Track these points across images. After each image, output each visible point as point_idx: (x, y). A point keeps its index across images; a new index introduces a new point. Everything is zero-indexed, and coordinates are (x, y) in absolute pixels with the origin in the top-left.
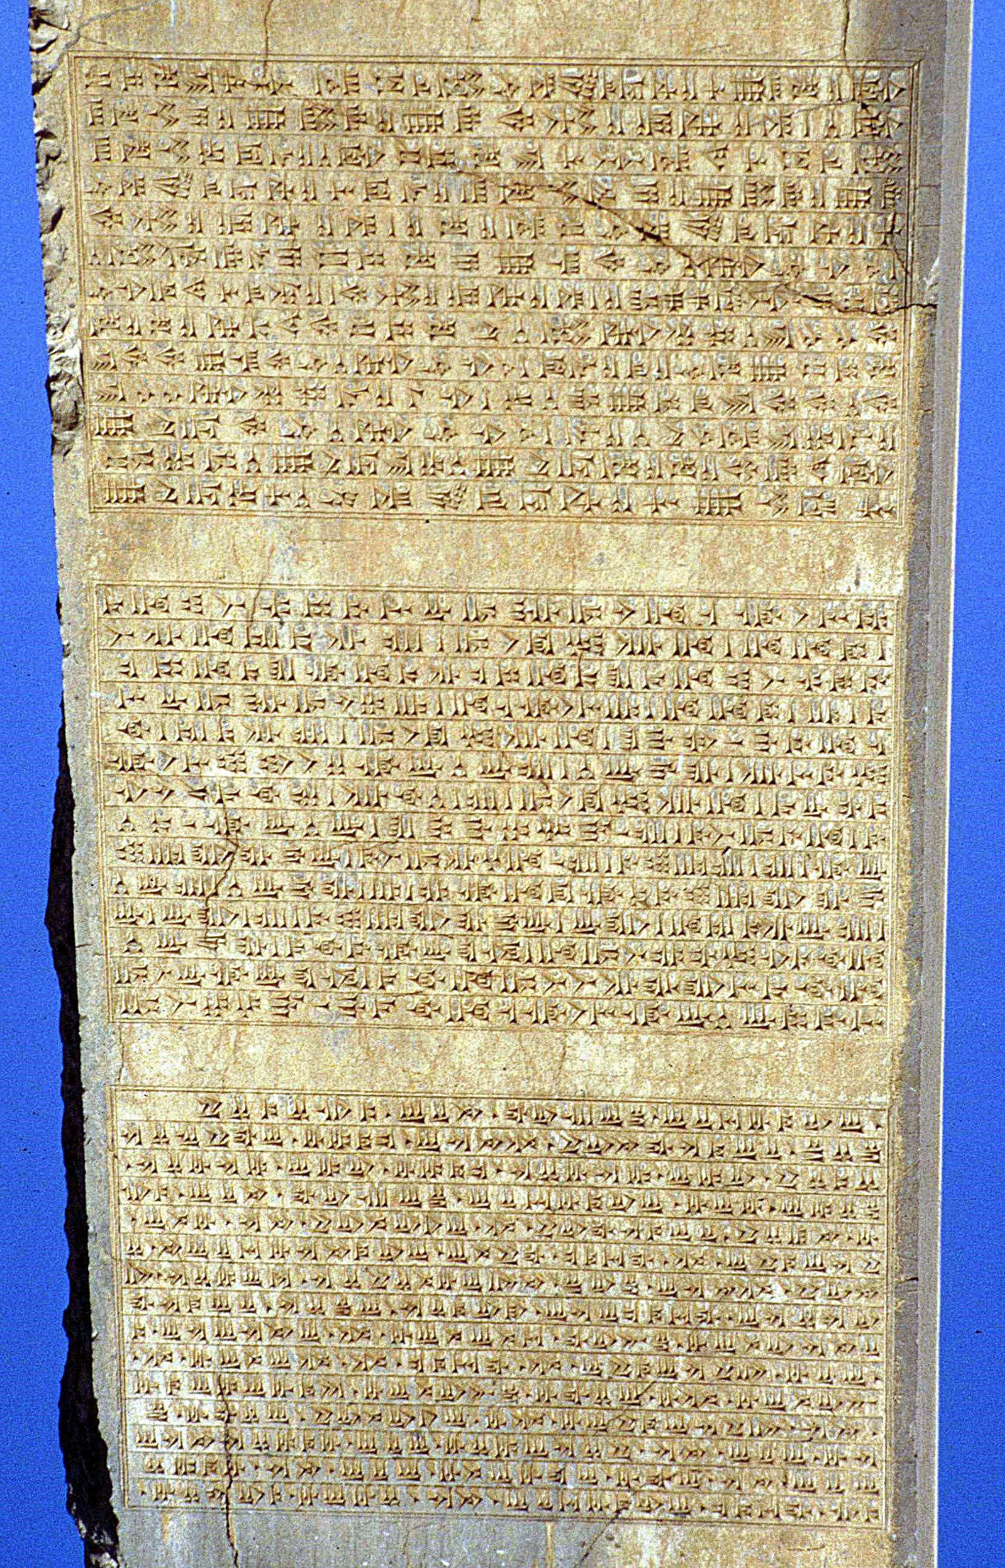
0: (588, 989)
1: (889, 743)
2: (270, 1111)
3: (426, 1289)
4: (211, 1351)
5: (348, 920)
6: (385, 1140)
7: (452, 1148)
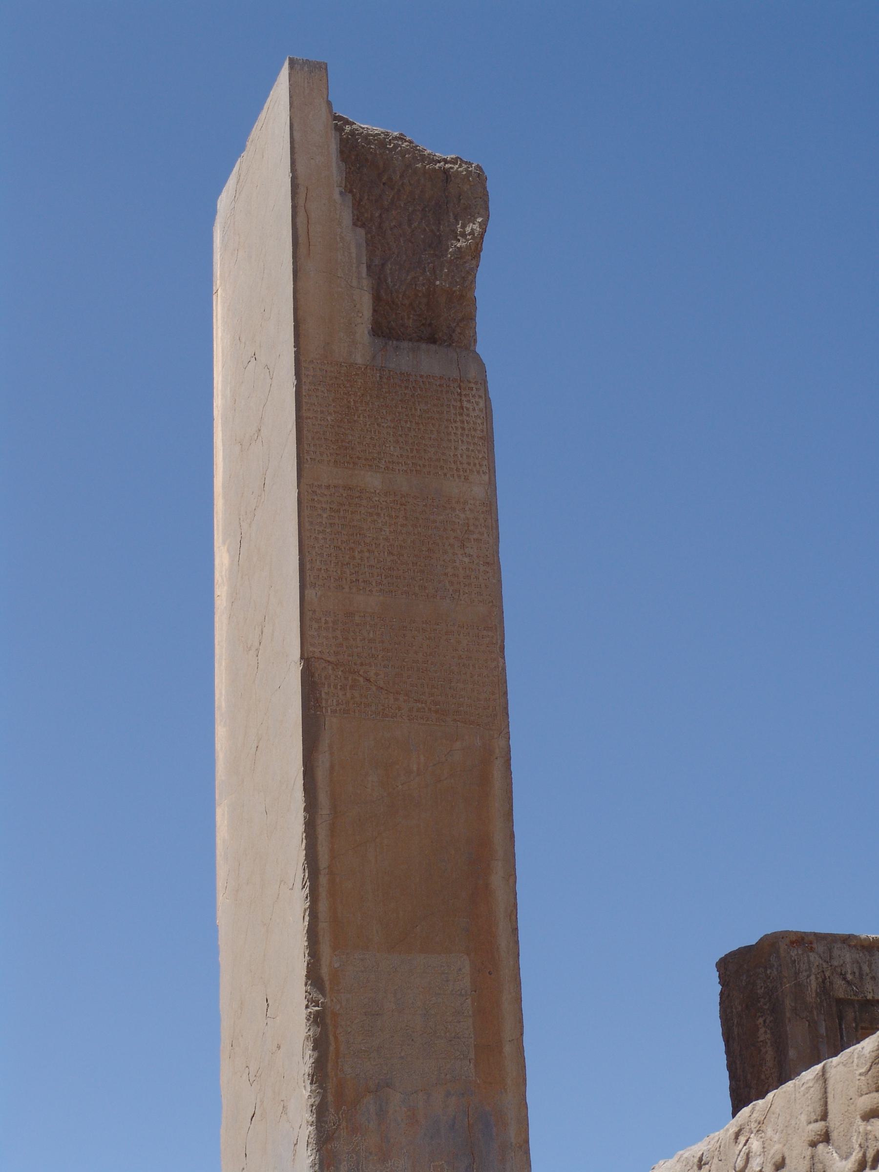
0: (377, 499)
1: (307, 554)
2: (453, 476)
3: (414, 428)
4: (465, 417)
5: (435, 521)
6: (424, 466)
7: (409, 463)
